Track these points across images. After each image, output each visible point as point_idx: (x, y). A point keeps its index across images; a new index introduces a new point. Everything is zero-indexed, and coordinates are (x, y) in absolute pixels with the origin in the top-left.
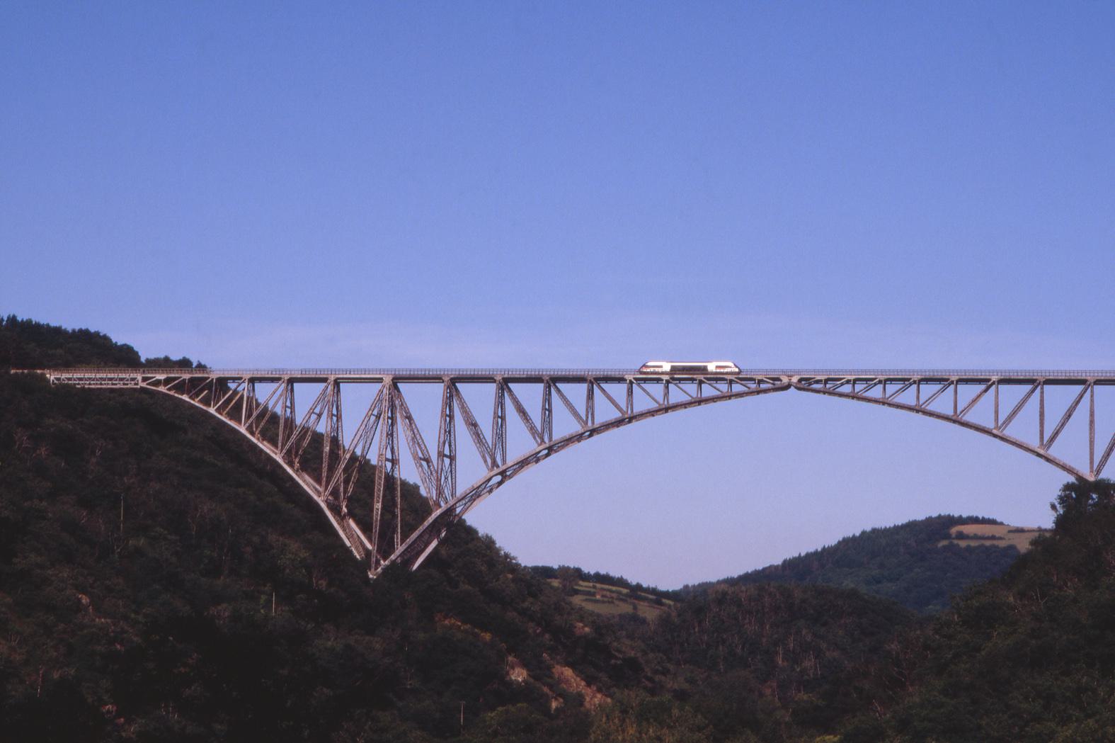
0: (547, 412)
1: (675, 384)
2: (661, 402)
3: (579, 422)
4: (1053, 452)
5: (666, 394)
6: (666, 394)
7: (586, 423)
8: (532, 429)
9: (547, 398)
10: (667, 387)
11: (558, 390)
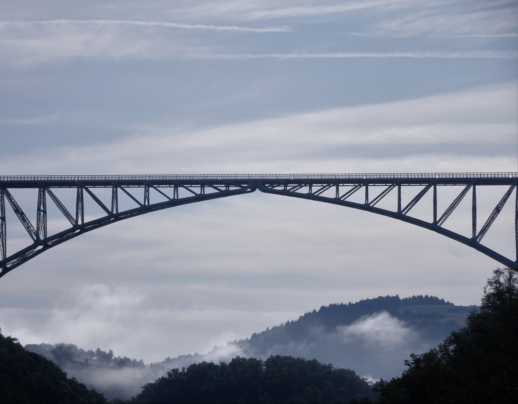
0: (42, 213)
1: (155, 188)
2: (143, 204)
3: (70, 221)
4: (484, 242)
5: (147, 197)
6: (147, 197)
7: (77, 221)
8: (28, 228)
9: (42, 201)
10: (147, 191)
11: (52, 195)
